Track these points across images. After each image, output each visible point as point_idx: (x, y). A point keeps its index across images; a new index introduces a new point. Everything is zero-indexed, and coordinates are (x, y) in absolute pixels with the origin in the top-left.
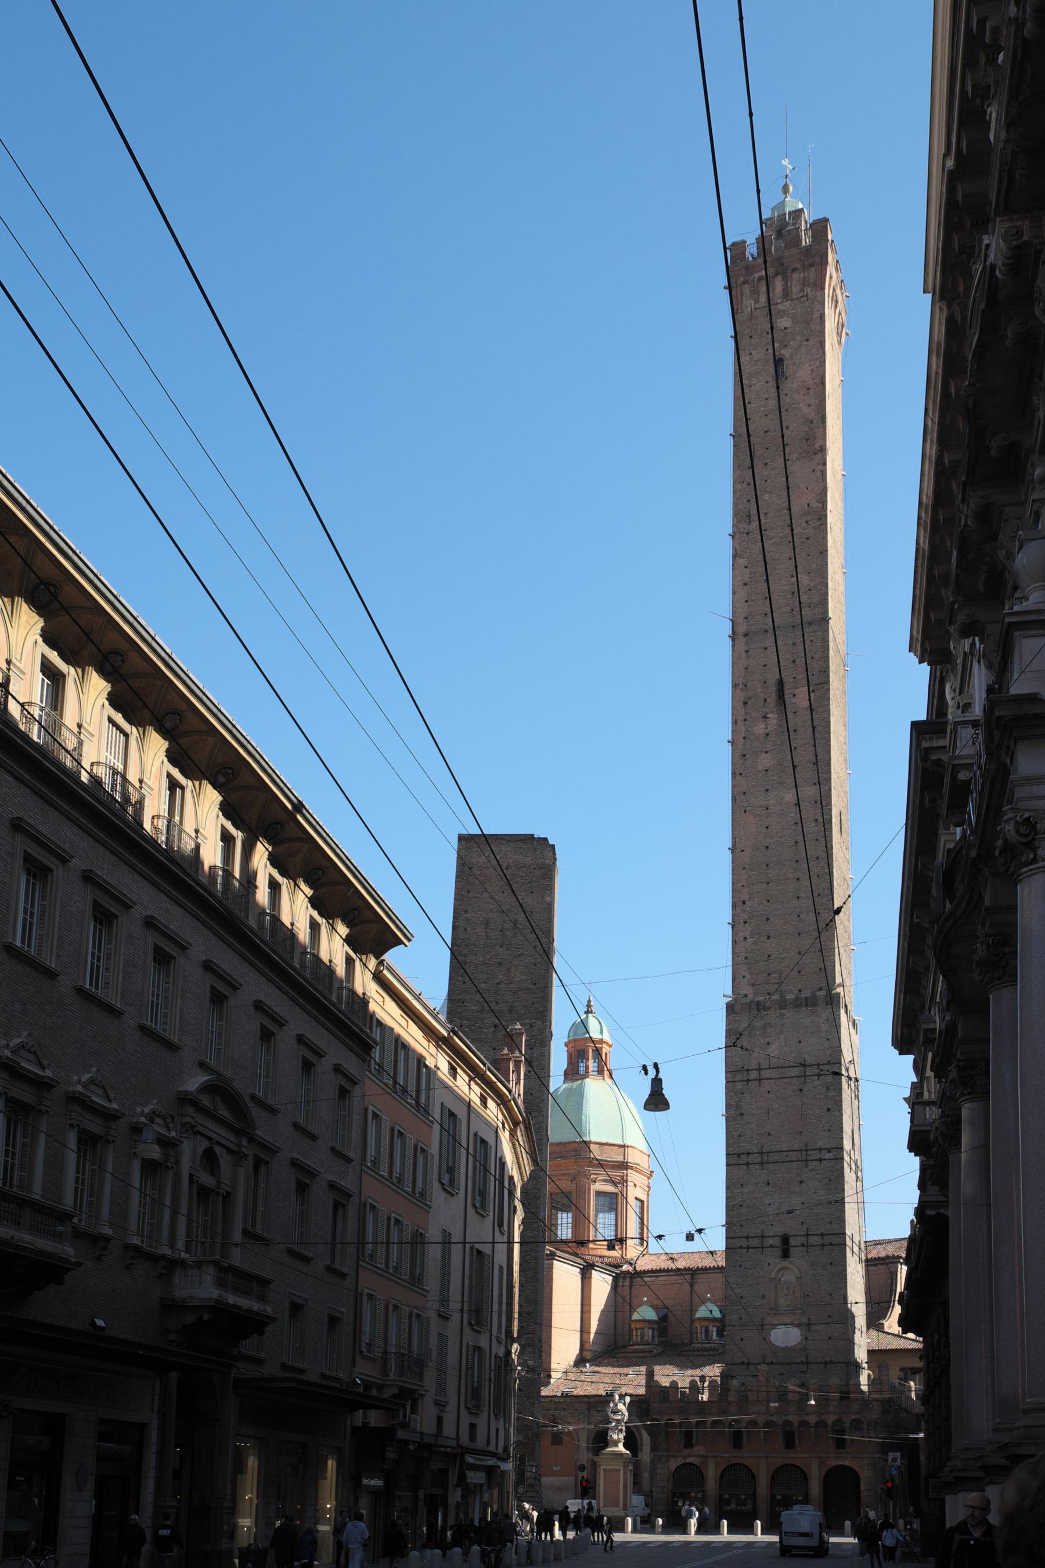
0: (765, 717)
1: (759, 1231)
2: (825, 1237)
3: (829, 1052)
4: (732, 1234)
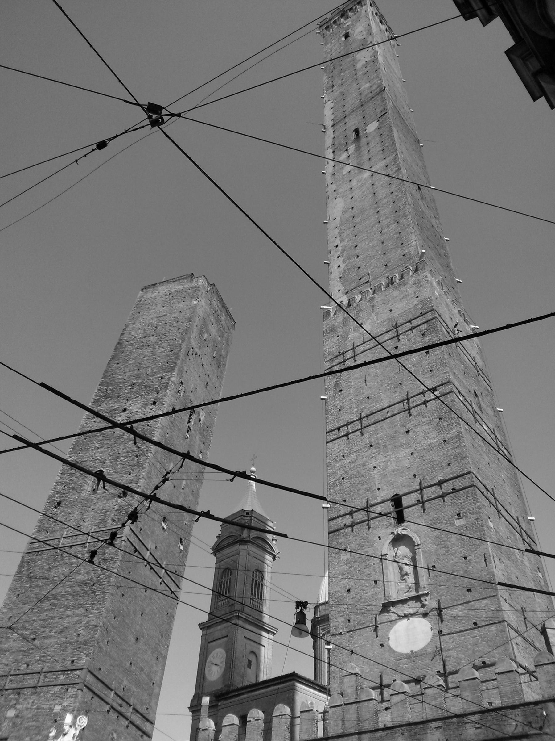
0: (347, 150)
1: (365, 501)
2: (444, 485)
3: (419, 306)
4: (332, 516)
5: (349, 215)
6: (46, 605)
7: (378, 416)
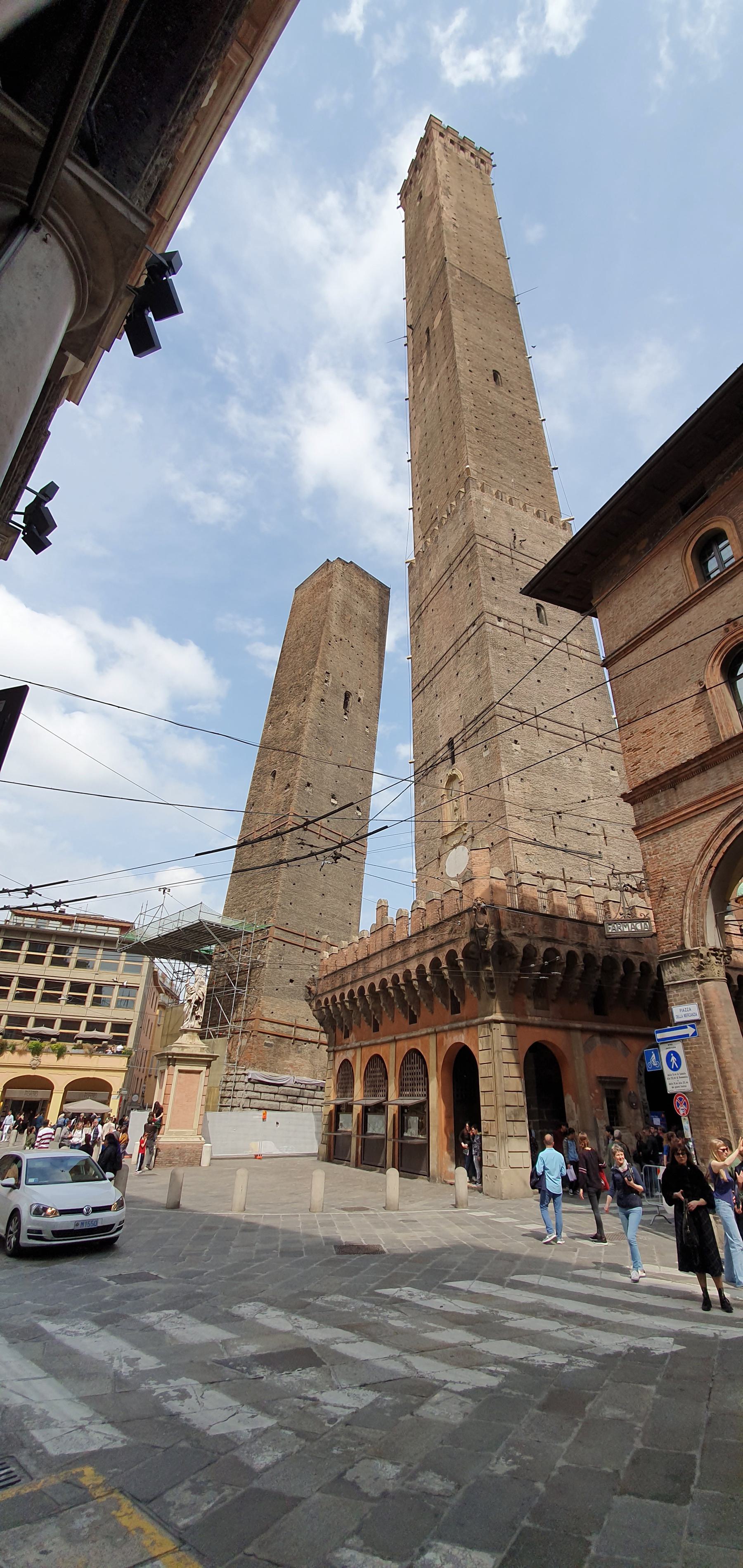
5: (424, 442)
6: (250, 885)
7: (441, 665)
